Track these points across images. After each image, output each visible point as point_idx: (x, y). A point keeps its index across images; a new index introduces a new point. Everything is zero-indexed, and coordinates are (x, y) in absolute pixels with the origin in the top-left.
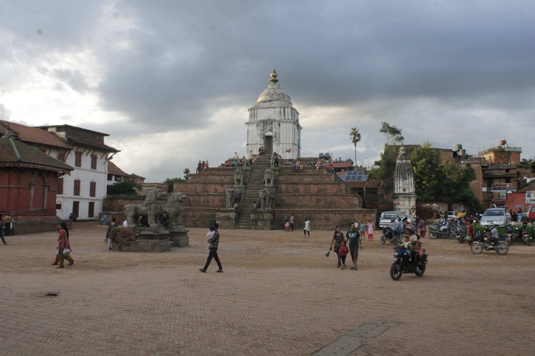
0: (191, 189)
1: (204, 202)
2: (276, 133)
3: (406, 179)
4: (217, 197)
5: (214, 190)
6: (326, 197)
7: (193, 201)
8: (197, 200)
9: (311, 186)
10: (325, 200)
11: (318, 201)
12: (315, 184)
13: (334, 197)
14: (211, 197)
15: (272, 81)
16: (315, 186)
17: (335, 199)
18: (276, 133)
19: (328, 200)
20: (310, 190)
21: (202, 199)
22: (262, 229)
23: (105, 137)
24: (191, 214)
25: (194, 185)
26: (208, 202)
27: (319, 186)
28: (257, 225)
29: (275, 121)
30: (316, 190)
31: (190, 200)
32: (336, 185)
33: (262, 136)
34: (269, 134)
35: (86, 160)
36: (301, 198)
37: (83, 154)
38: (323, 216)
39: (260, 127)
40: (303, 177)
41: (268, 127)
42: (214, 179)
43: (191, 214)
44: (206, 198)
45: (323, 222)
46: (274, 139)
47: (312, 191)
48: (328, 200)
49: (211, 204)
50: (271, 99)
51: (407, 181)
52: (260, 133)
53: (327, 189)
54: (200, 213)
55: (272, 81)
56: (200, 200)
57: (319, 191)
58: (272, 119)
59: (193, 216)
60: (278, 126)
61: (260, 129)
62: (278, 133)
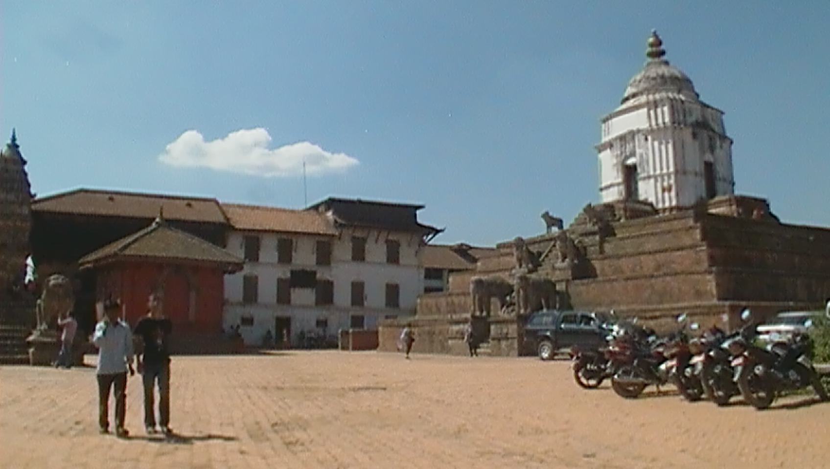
6: (653, 281)
8: (462, 302)
9: (642, 258)
10: (652, 286)
12: (650, 253)
13: (668, 278)
15: (651, 55)
16: (651, 257)
18: (641, 156)
20: (641, 268)
22: (508, 355)
23: (418, 212)
27: (657, 256)
29: (639, 131)
30: (652, 264)
32: (689, 250)
33: (620, 167)
34: (630, 162)
35: (376, 250)
36: (608, 286)
37: (368, 240)
40: (642, 240)
46: (639, 170)
47: (645, 269)
52: (615, 161)
55: (651, 55)
57: (658, 267)
62: (644, 156)
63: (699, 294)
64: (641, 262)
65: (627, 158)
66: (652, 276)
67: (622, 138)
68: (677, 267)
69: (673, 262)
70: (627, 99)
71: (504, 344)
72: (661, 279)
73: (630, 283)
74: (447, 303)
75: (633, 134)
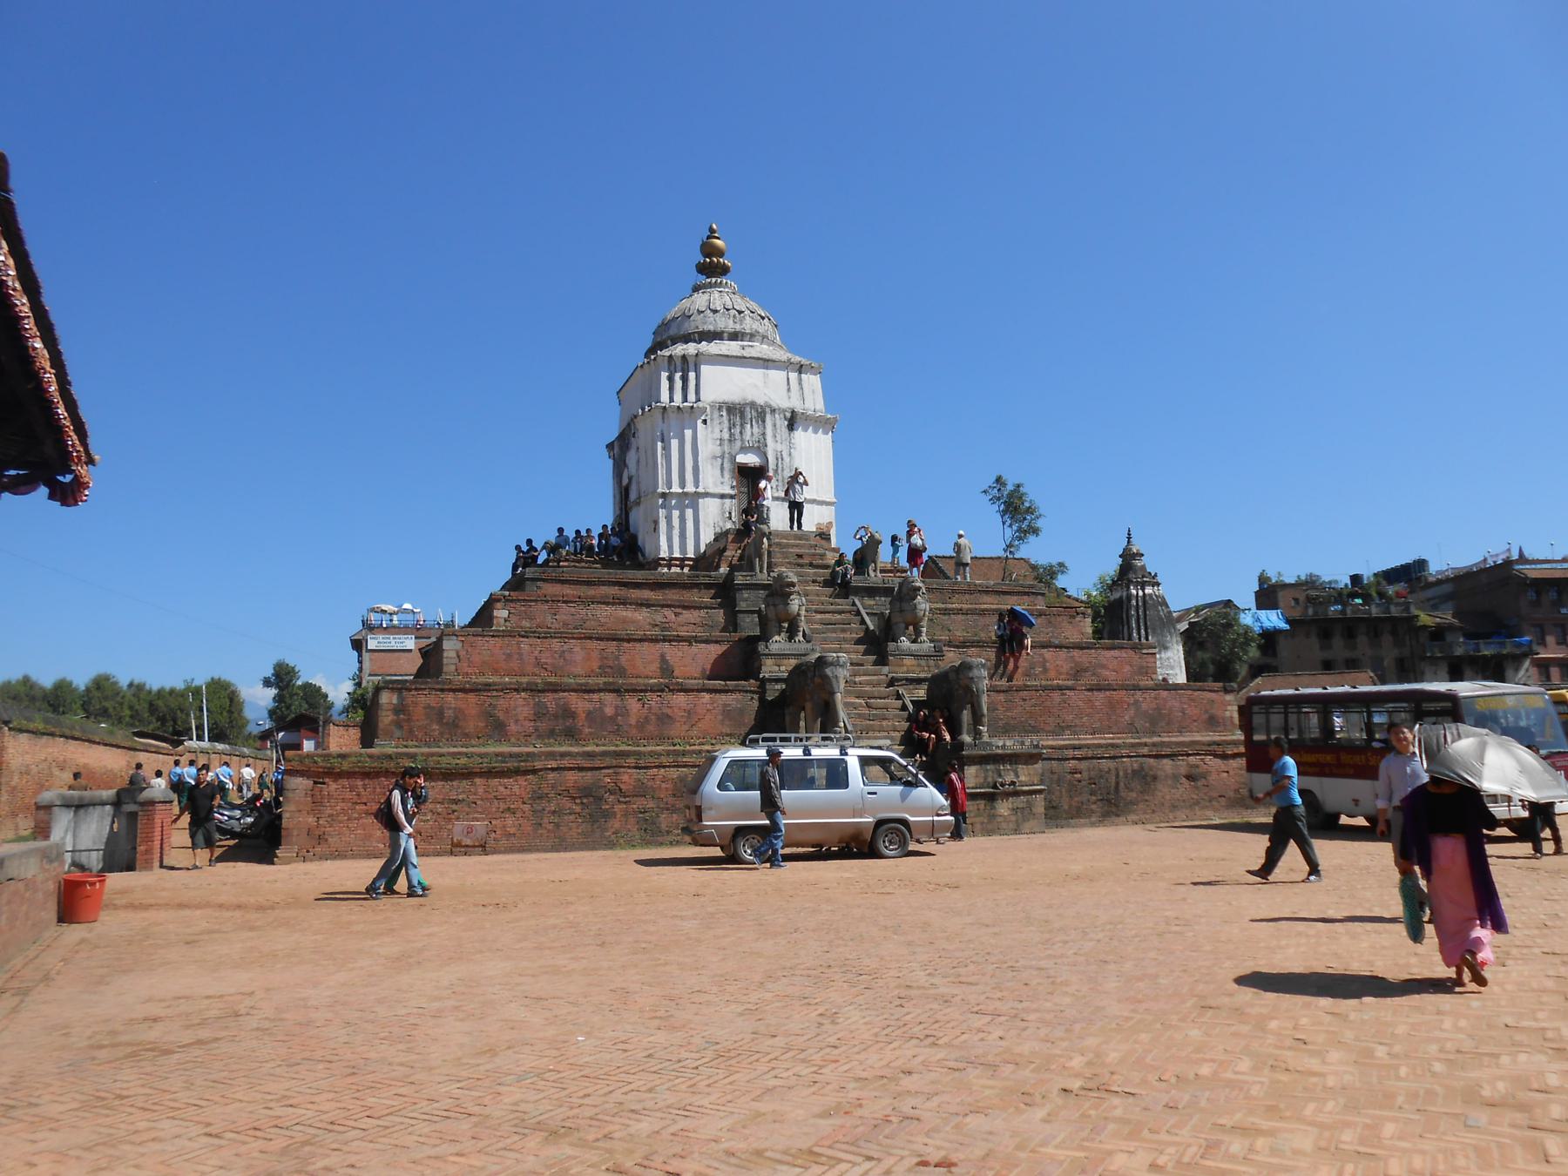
0: (538, 664)
1: (641, 726)
2: (779, 457)
3: (1166, 648)
4: (706, 697)
5: (655, 667)
7: (589, 713)
8: (609, 711)
11: (1112, 705)
12: (1060, 647)
14: (680, 699)
16: (1063, 653)
17: (1165, 700)
19: (1144, 706)
20: (1045, 670)
21: (632, 703)
22: (1017, 831)
24: (628, 778)
25: (556, 644)
26: (665, 719)
27: (1076, 653)
28: (992, 817)
29: (773, 411)
30: (1066, 667)
31: (571, 714)
33: (727, 465)
34: (751, 459)
36: (1056, 696)
38: (1182, 765)
39: (717, 430)
41: (751, 432)
42: (625, 621)
43: (628, 778)
44: (653, 700)
45: (1184, 789)
47: (1052, 674)
48: (1144, 706)
49: (678, 729)
50: (738, 327)
51: (1169, 654)
53: (1104, 667)
54: (674, 773)
56: (622, 711)
57: (1078, 672)
58: (760, 401)
59: (641, 791)
60: (785, 430)
61: (717, 435)
63: (1213, 722)
64: (1045, 661)
65: (744, 450)
66: (1136, 688)
67: (736, 412)
68: (1110, 676)
69: (1104, 667)
70: (715, 336)
71: (1003, 808)
72: (1153, 693)
73: (1100, 695)
74: (539, 714)
75: (762, 413)
